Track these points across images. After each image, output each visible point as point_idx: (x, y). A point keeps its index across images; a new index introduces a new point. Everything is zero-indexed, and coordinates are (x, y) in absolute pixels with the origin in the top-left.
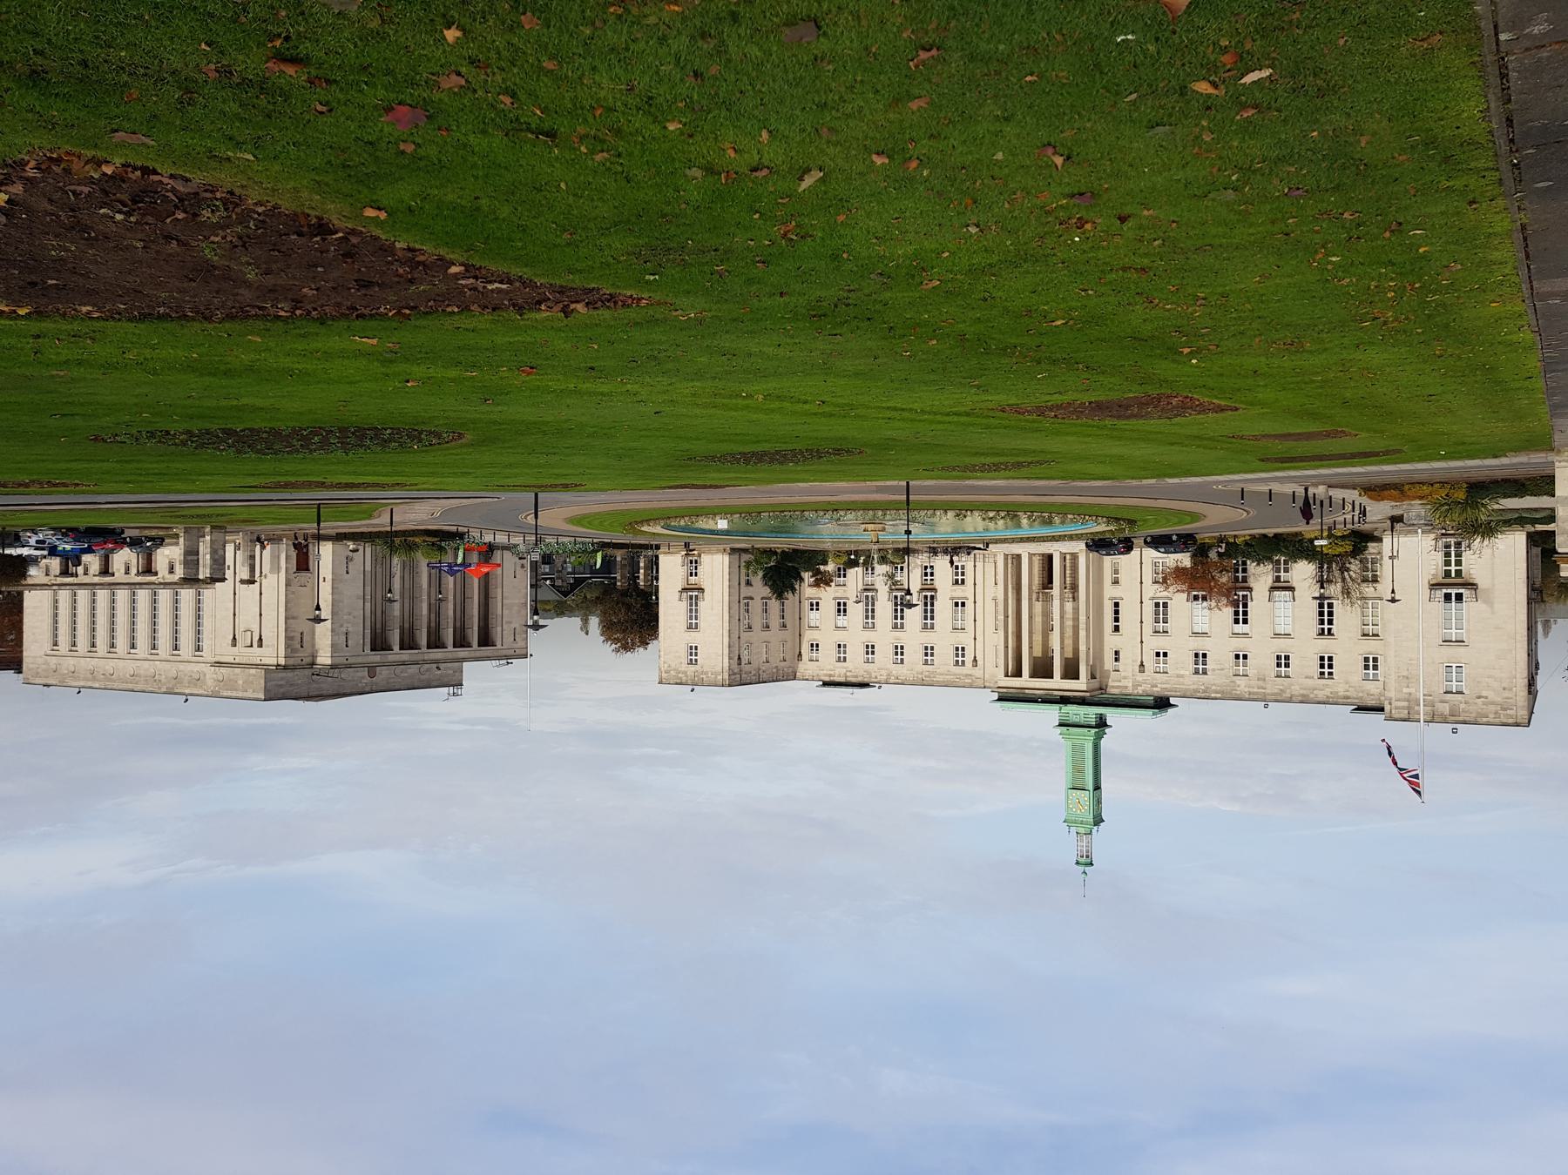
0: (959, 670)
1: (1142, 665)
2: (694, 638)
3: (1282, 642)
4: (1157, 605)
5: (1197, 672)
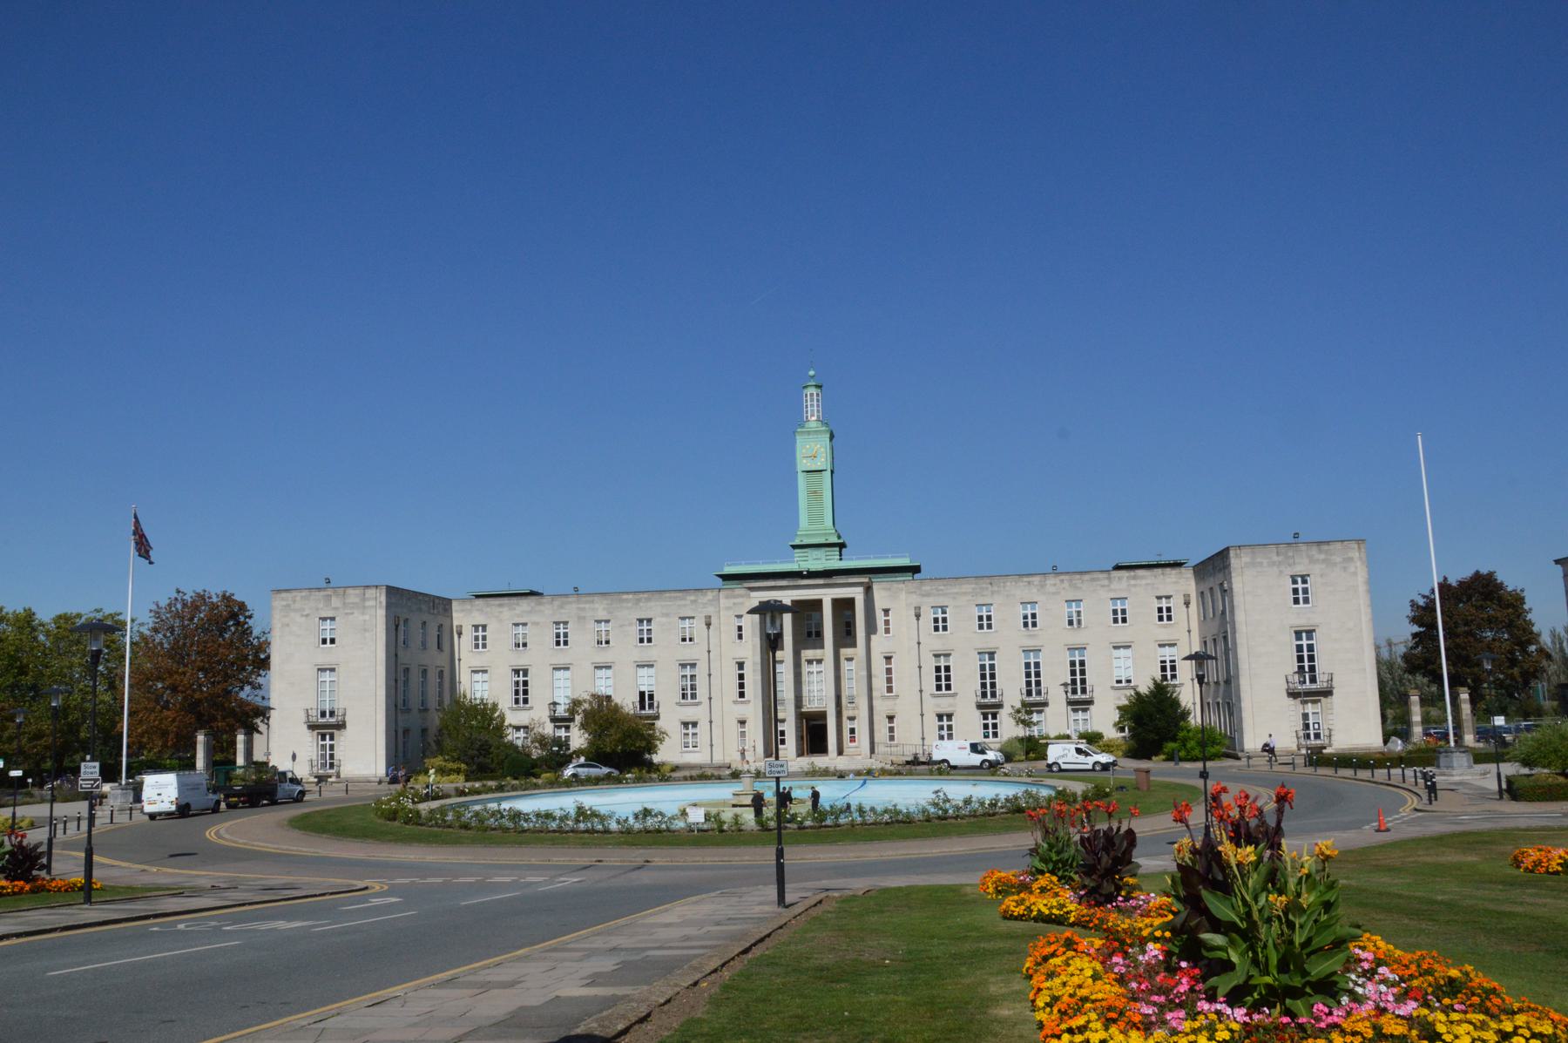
0: (941, 601)
1: (708, 625)
2: (1301, 616)
3: (561, 660)
4: (694, 696)
5: (649, 621)
